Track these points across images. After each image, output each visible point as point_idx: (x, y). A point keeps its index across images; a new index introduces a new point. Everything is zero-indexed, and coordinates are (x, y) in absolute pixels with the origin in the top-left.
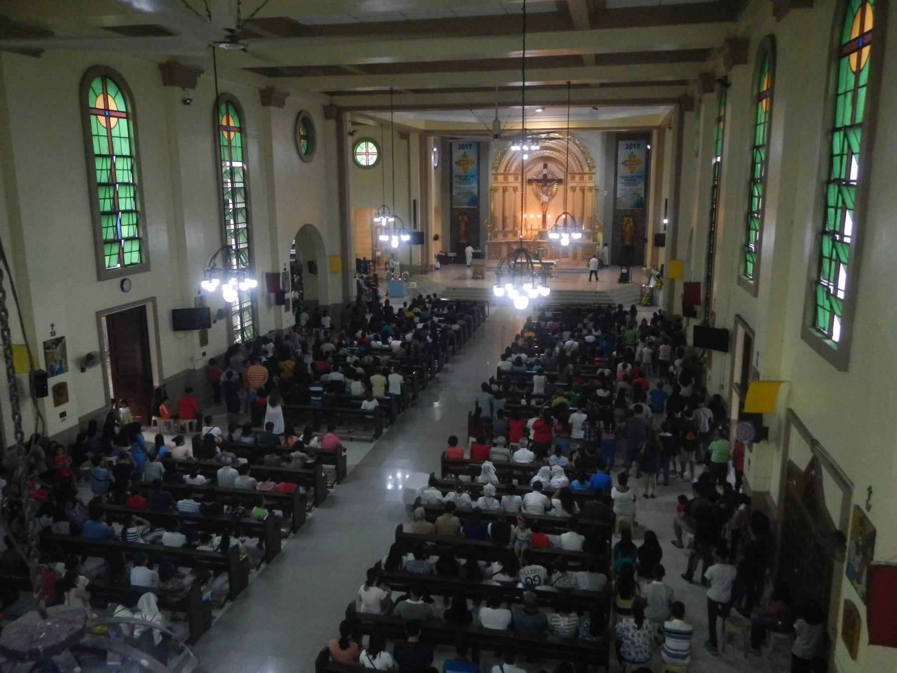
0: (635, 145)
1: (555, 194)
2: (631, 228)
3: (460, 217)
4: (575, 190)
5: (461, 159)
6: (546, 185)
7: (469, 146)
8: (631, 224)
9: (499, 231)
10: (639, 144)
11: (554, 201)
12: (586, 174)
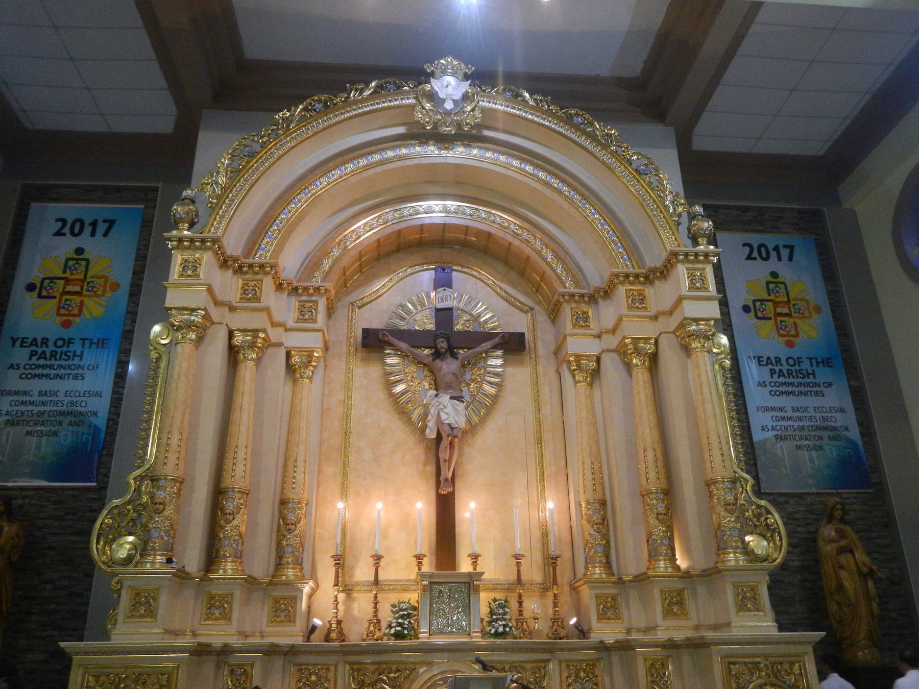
1: (495, 398)
4: (596, 373)
5: (61, 275)
6: (454, 356)
7: (101, 228)
8: (861, 556)
10: (791, 248)
11: (488, 435)
12: (663, 272)
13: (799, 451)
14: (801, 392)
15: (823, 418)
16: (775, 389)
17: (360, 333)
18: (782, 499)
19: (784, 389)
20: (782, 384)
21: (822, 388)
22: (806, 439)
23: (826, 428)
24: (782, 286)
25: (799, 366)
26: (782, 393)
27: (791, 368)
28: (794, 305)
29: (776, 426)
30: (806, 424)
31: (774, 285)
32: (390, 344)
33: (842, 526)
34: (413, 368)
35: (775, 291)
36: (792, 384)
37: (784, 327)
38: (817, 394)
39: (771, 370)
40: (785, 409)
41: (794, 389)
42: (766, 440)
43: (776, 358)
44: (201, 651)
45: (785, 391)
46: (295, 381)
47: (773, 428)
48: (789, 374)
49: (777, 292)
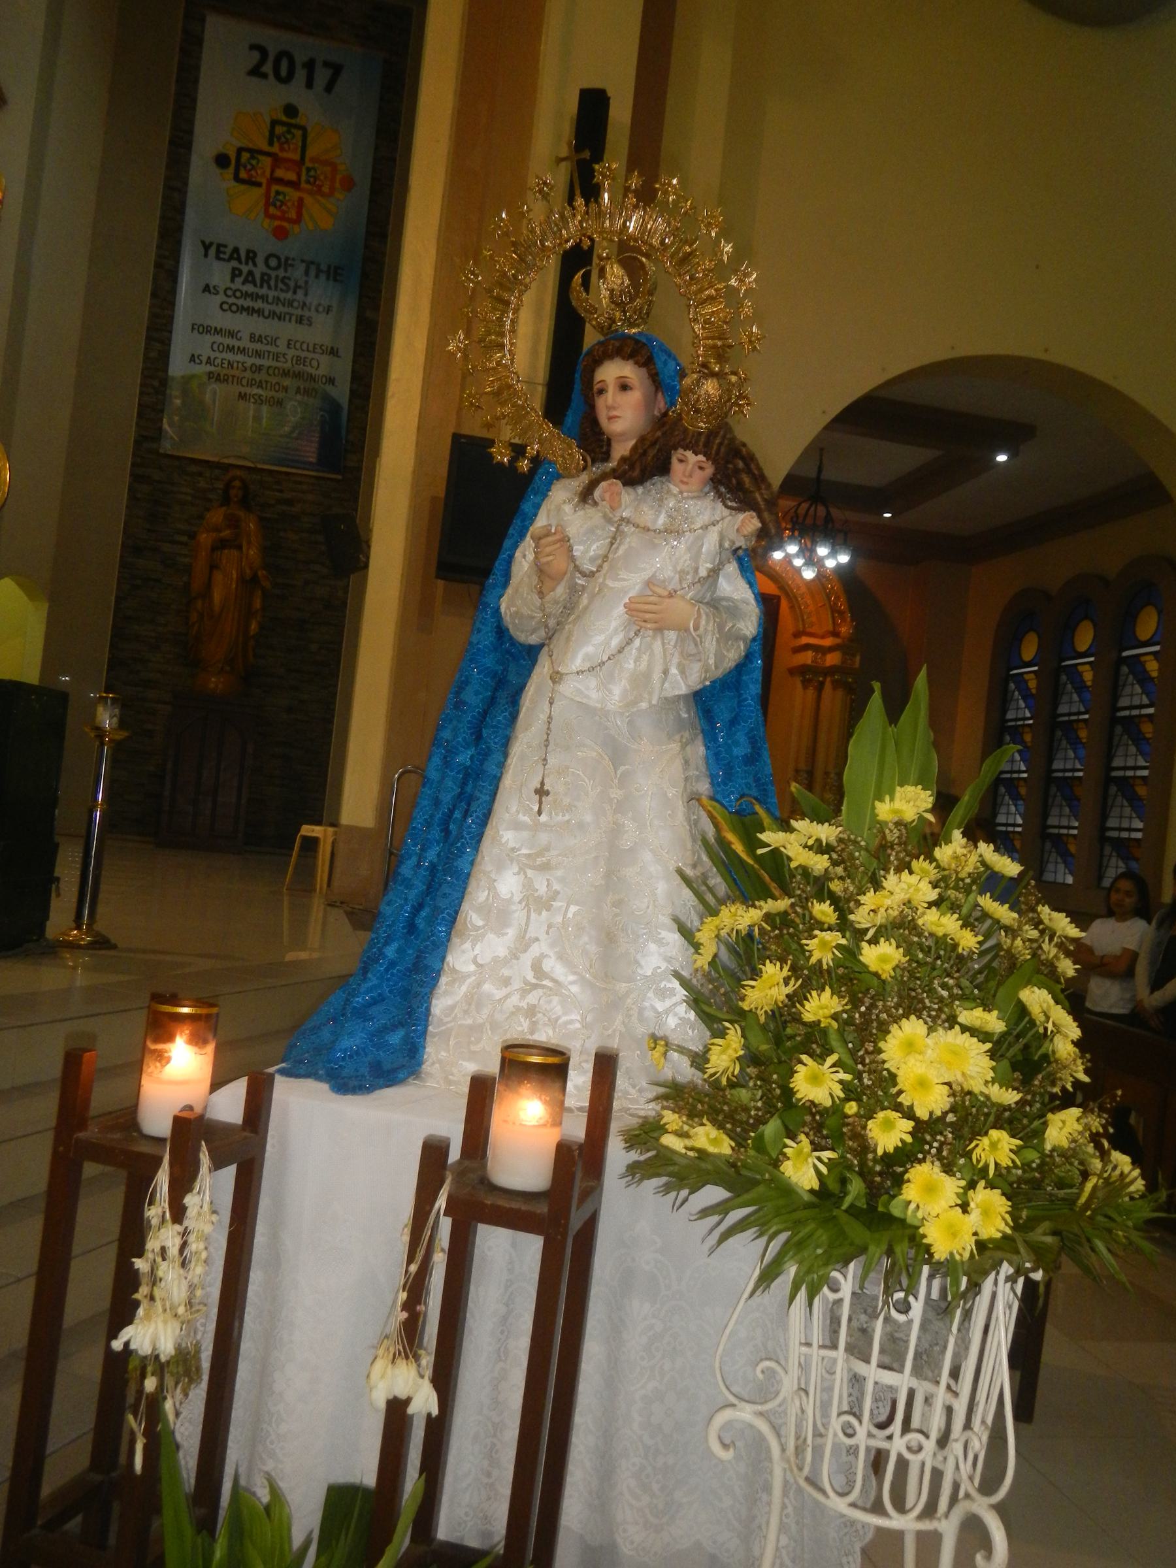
0: (310, 66)
2: (249, 583)
13: (241, 404)
14: (274, 313)
15: (298, 358)
16: (231, 300)
18: (193, 468)
19: (248, 303)
20: (246, 295)
21: (313, 314)
22: (260, 386)
23: (298, 375)
24: (298, 133)
25: (286, 271)
26: (242, 309)
27: (269, 272)
28: (308, 170)
29: (215, 358)
30: (266, 363)
31: (285, 129)
33: (241, 514)
35: (283, 139)
36: (264, 298)
37: (278, 204)
38: (300, 320)
39: (234, 269)
40: (239, 335)
41: (267, 308)
42: (193, 377)
43: (248, 252)
45: (249, 307)
47: (209, 361)
48: (262, 280)
49: (287, 141)
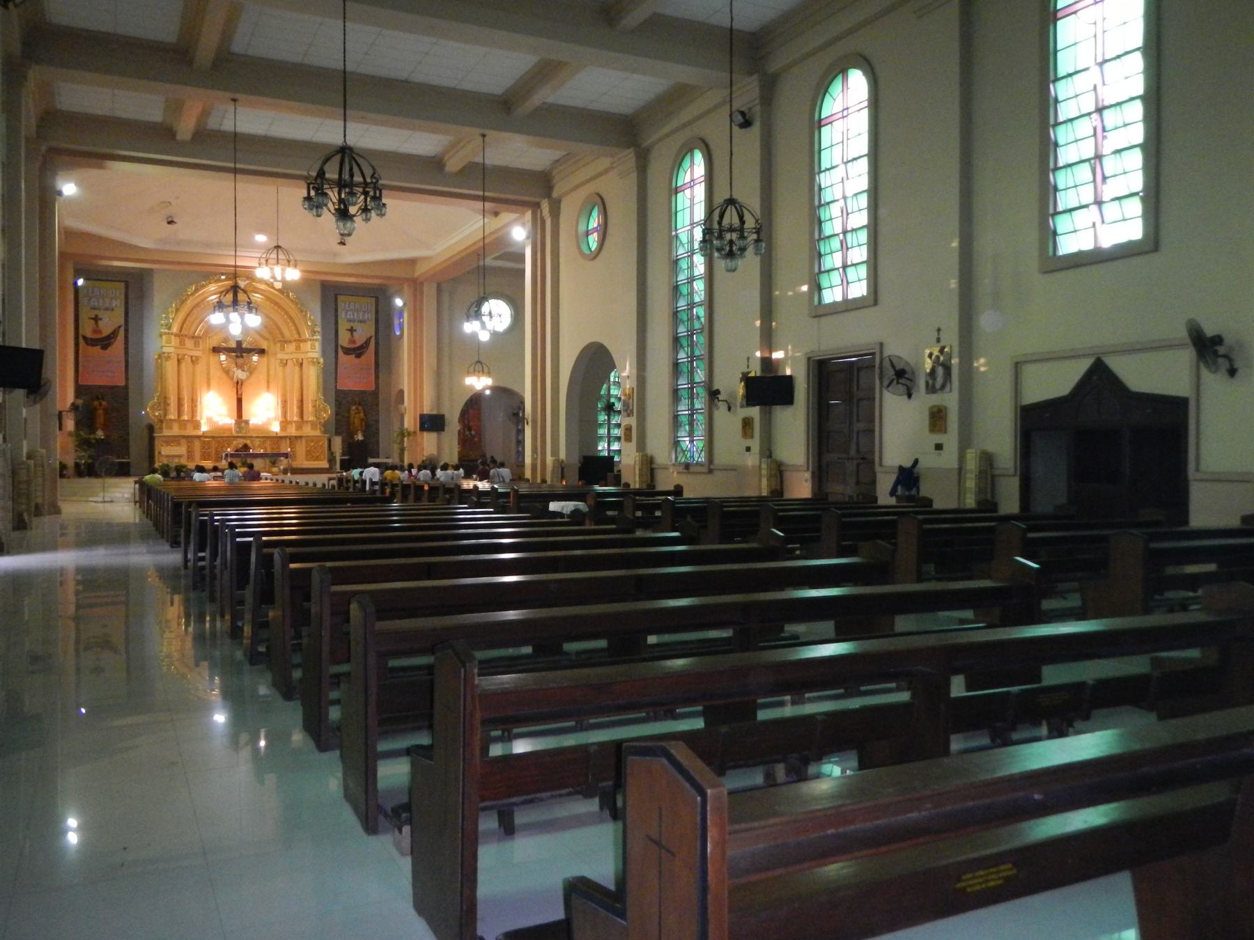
3: (96, 403)
4: (286, 364)
6: (242, 357)
8: (362, 415)
9: (174, 420)
12: (305, 341)
17: (211, 348)
32: (221, 352)
34: (229, 360)
44: (184, 437)
46: (193, 364)
